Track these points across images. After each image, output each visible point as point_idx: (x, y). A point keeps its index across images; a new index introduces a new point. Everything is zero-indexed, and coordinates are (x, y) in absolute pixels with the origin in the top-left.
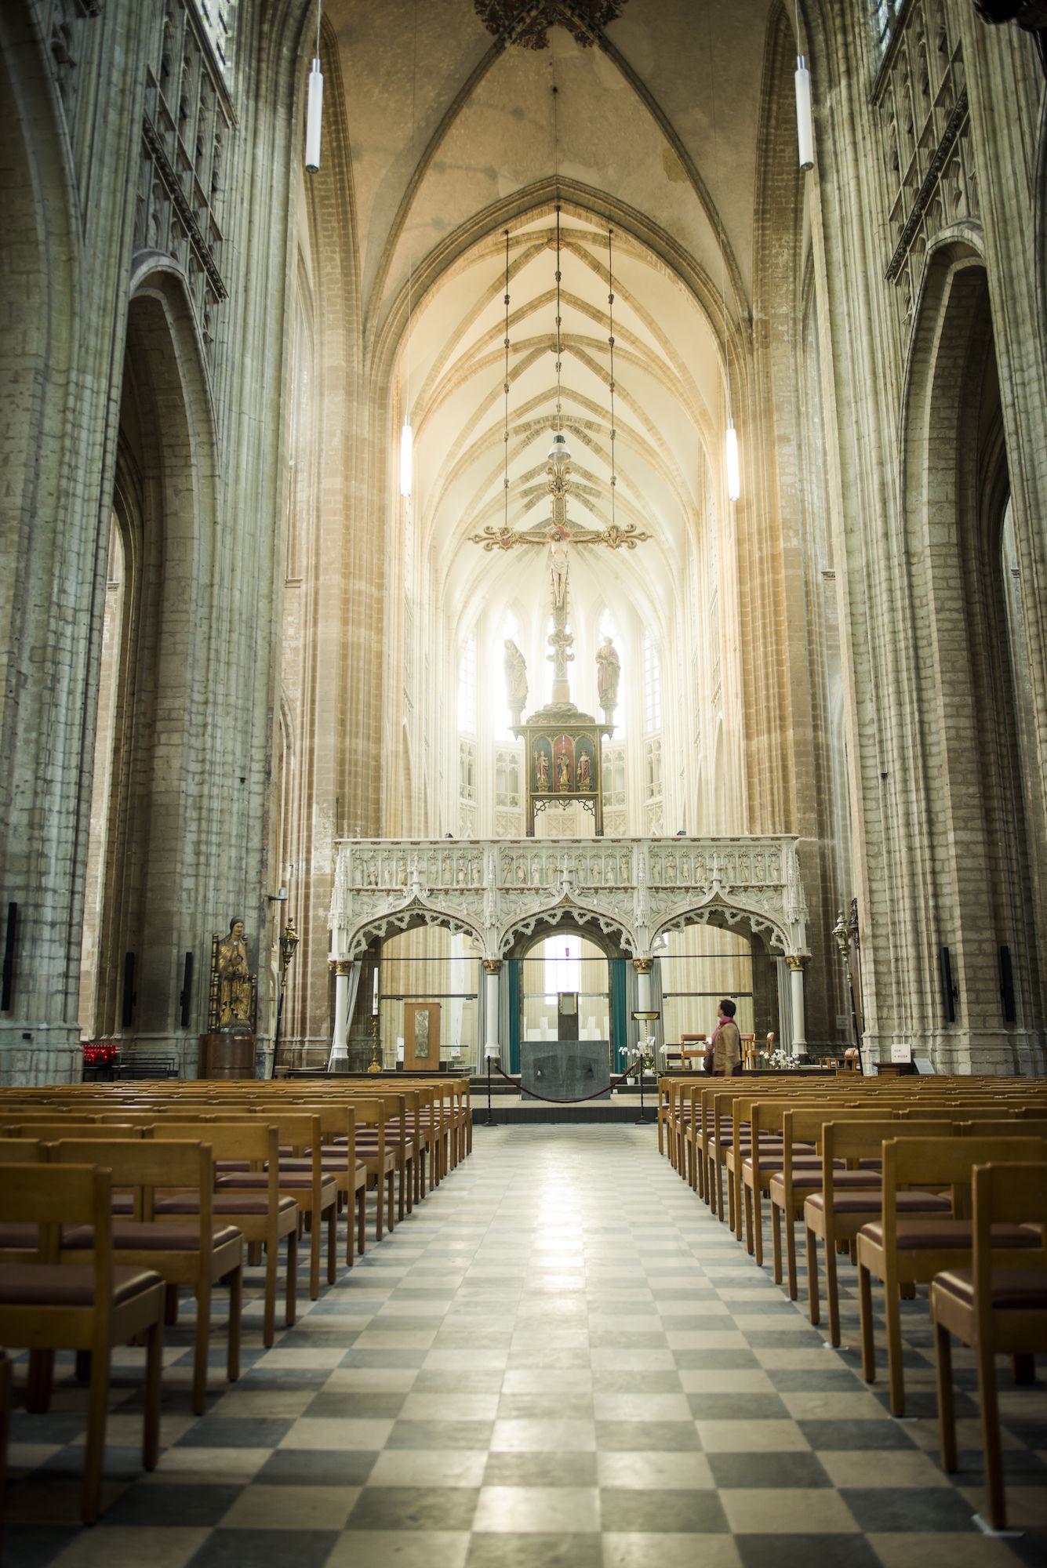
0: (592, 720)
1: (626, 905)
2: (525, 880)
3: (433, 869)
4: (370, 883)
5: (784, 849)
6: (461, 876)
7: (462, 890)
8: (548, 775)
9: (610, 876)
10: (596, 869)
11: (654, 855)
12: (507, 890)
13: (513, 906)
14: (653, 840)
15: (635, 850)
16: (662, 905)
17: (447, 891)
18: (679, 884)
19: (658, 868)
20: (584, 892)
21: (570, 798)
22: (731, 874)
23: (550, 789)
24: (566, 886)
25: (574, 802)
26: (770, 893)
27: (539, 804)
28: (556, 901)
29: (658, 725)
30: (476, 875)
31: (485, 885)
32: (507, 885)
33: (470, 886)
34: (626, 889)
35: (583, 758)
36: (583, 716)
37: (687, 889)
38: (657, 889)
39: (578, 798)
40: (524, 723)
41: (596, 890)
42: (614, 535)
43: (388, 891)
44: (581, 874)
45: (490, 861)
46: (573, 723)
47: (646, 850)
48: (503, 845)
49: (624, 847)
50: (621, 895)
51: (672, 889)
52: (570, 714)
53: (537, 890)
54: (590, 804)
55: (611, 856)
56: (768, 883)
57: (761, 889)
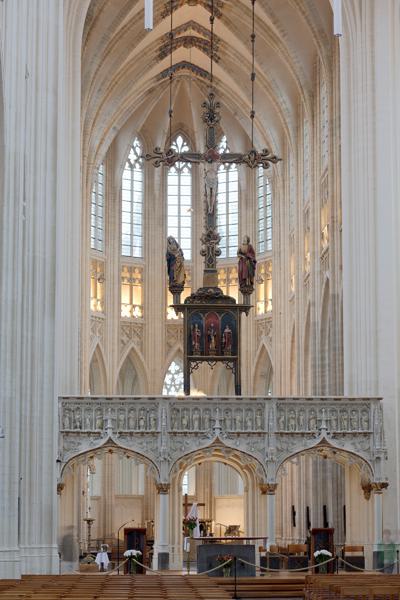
0: (234, 301)
1: (262, 446)
2: (188, 427)
3: (122, 417)
4: (76, 427)
5: (373, 406)
6: (142, 423)
7: (142, 433)
8: (201, 344)
9: (249, 424)
10: (238, 418)
11: (279, 409)
12: (175, 433)
13: (179, 445)
14: (279, 399)
15: (267, 406)
16: (285, 446)
17: (131, 434)
18: (297, 431)
19: (282, 419)
20: (230, 436)
21: (216, 360)
22: (334, 423)
23: (202, 354)
24: (217, 432)
25: (220, 363)
26: (361, 438)
27: (193, 364)
28: (209, 443)
29: (270, 247)
30: (153, 423)
31: (159, 430)
32: (175, 430)
33: (148, 431)
34: (259, 434)
35: (227, 330)
36: (228, 298)
37: (303, 434)
38: (282, 434)
39: (222, 360)
40: (182, 302)
41: (239, 434)
42: (253, 157)
43: (89, 433)
44: (228, 423)
45: (163, 411)
46: (220, 303)
47: (274, 406)
48: (173, 401)
49: (258, 405)
50: (255, 438)
51: (292, 434)
52: (218, 296)
53: (196, 433)
54: (231, 364)
55: (250, 410)
56: (360, 431)
57: (354, 435)
